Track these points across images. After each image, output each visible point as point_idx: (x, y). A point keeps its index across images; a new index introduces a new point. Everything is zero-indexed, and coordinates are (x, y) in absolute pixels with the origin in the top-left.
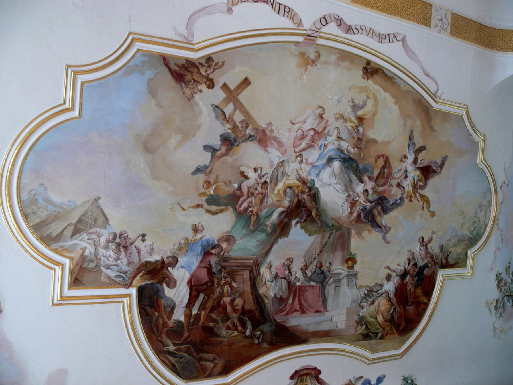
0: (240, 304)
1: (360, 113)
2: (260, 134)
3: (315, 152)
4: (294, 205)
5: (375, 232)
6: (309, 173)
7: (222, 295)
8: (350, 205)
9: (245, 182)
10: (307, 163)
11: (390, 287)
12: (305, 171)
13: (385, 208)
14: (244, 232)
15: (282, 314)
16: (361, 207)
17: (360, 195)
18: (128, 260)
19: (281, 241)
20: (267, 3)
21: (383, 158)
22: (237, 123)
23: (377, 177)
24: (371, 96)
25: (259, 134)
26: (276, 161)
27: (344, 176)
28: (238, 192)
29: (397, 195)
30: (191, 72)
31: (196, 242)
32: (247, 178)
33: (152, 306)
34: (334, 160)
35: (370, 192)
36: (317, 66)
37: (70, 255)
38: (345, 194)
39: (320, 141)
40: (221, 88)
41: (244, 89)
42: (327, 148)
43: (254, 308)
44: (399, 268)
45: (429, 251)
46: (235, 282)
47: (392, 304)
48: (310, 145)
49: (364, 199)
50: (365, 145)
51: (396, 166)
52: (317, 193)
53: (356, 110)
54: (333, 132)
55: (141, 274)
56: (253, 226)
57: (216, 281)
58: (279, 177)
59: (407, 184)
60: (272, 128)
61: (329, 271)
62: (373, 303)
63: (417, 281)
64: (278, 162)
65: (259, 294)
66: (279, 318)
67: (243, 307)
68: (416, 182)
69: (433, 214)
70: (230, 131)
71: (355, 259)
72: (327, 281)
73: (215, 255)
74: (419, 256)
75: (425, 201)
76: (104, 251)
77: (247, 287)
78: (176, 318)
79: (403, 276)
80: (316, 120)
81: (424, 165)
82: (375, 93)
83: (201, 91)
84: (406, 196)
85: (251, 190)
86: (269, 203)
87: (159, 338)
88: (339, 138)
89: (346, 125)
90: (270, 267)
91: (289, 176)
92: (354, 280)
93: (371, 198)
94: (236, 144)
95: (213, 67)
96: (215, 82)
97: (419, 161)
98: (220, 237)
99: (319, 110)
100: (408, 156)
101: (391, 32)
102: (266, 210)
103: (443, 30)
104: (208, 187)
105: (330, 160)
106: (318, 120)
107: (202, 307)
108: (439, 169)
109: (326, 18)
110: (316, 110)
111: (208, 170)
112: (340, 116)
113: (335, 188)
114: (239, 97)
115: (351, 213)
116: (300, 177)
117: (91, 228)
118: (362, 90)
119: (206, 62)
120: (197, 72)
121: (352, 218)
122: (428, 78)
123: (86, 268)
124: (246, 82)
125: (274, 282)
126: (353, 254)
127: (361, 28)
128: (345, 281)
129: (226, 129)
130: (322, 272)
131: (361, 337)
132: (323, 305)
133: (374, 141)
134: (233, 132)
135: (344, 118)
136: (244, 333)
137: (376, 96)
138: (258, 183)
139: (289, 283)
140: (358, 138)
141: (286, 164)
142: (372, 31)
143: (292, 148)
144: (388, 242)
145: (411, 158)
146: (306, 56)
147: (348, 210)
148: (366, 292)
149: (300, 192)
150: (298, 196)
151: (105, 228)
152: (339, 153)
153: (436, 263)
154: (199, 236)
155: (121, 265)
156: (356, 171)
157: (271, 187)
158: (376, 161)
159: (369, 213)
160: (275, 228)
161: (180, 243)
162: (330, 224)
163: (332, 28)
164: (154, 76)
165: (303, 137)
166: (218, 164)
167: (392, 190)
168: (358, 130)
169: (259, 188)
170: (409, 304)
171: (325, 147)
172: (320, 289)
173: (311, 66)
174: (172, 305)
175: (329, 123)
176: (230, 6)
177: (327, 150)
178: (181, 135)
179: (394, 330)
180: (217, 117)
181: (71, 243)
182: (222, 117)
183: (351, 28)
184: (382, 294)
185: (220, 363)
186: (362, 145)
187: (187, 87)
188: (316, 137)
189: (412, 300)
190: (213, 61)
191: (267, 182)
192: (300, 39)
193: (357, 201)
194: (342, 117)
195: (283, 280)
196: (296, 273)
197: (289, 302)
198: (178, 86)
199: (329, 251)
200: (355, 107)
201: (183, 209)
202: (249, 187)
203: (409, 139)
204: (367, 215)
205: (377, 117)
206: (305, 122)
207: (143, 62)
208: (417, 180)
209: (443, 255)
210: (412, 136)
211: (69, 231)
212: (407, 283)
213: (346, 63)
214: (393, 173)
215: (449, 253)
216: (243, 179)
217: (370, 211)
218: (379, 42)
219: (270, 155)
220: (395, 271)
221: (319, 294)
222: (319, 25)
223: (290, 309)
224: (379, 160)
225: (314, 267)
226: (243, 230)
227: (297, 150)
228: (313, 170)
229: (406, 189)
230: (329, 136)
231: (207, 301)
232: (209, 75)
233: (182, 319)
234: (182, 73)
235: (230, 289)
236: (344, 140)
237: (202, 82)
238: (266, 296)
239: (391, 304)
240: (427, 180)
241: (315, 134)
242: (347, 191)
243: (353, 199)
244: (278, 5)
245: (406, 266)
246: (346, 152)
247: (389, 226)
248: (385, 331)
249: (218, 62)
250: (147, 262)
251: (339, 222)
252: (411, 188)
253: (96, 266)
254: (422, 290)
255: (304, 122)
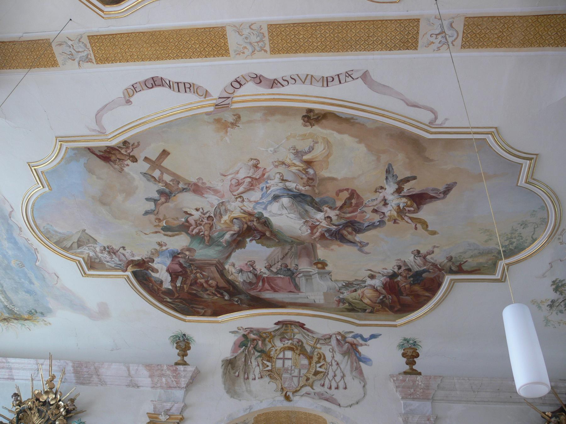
0: (214, 283)
1: (306, 157)
2: (193, 187)
3: (256, 193)
4: (244, 229)
5: (346, 246)
6: (254, 208)
7: (196, 279)
8: (309, 228)
9: (190, 218)
10: (250, 201)
11: (377, 282)
12: (249, 207)
13: (357, 229)
14: (201, 246)
15: (254, 291)
16: (324, 229)
17: (321, 221)
18: (119, 259)
19: (238, 251)
20: (163, 86)
21: (348, 192)
22: (168, 182)
23: (341, 208)
24: (320, 140)
25: (191, 186)
26: (216, 203)
27: (297, 208)
28: (187, 224)
29: (373, 219)
30: (114, 154)
31: (163, 251)
32: (191, 215)
33: (146, 280)
34: (281, 197)
35: (334, 218)
36: (238, 126)
37: (82, 256)
38: (301, 220)
39: (260, 185)
40: (143, 160)
41: (164, 159)
42: (270, 189)
43: (227, 286)
44: (385, 271)
45: (428, 261)
46: (205, 272)
47: (380, 293)
48: (249, 189)
49: (327, 223)
50: (318, 183)
51: (368, 197)
52: (268, 221)
53: (300, 155)
54: (274, 177)
55: (131, 265)
56: (208, 242)
57: (188, 270)
58: (222, 212)
59: (390, 211)
60: (203, 181)
61: (297, 270)
62: (355, 291)
63: (413, 281)
64: (218, 203)
65: (228, 279)
66: (253, 293)
67: (217, 285)
68: (401, 208)
69: (434, 233)
70: (164, 188)
71: (325, 263)
72: (295, 275)
73: (182, 257)
74: (413, 264)
75: (420, 223)
76: (102, 255)
77: (217, 275)
78: (165, 287)
79: (394, 276)
80: (250, 170)
81: (414, 193)
82: (325, 137)
83: (128, 165)
84: (388, 219)
85: (198, 222)
86: (218, 229)
87: (158, 295)
88: (283, 180)
89: (290, 169)
90: (233, 265)
91: (232, 211)
92: (328, 276)
93: (337, 223)
94: (173, 195)
95: (131, 148)
96: (136, 157)
97: (405, 190)
98: (182, 248)
99: (252, 162)
100: (387, 187)
101: (342, 70)
102: (217, 233)
103: (445, 47)
104: (160, 222)
105: (276, 198)
106: (252, 170)
107: (183, 283)
108: (442, 195)
109: (239, 81)
110: (248, 162)
111: (156, 212)
112: (280, 163)
113: (288, 217)
114: (162, 164)
115: (312, 233)
116: (245, 211)
117: (87, 244)
118: (304, 137)
119: (124, 145)
120: (119, 153)
121: (315, 236)
122: (416, 108)
123: (94, 262)
124: (165, 153)
125: (240, 274)
126: (321, 260)
127: (292, 78)
128: (317, 275)
129: (161, 186)
130: (289, 270)
131: (344, 310)
132: (295, 288)
133: (332, 179)
134: (167, 188)
135: (285, 165)
136: (224, 298)
137: (327, 139)
138: (203, 218)
139: (256, 275)
140: (309, 178)
141: (227, 204)
142: (309, 77)
143: (230, 192)
144: (367, 253)
145: (391, 188)
146: (223, 121)
147: (307, 232)
148: (344, 284)
149: (248, 221)
150: (247, 223)
151: (97, 244)
152: (285, 191)
153: (440, 270)
154: (164, 248)
155: (115, 261)
156: (311, 203)
157: (217, 219)
158: (337, 194)
159: (336, 233)
160: (229, 244)
161: (152, 252)
162: (290, 241)
163: (250, 88)
164: (87, 161)
165: (239, 184)
166: (162, 209)
167: (366, 216)
168: (307, 172)
169: (205, 221)
170: (404, 295)
171: (268, 189)
172: (290, 279)
173: (232, 128)
174: (160, 281)
175: (268, 170)
176: (127, 98)
177: (270, 191)
178: (125, 194)
179: (387, 309)
180: (148, 180)
181: (79, 250)
182: (153, 180)
183: (276, 82)
184: (365, 286)
185: (209, 311)
186: (316, 183)
187: (115, 164)
188: (255, 182)
189: (408, 293)
190: (129, 143)
191: (212, 217)
192: (211, 109)
193: (318, 225)
194: (283, 163)
195: (249, 273)
196: (261, 270)
197: (259, 285)
198: (108, 164)
199: (293, 257)
200: (298, 153)
201: (145, 234)
202: (195, 220)
203: (387, 172)
204: (334, 235)
205: (331, 158)
206: (238, 173)
207: (75, 154)
208: (403, 207)
209: (453, 263)
210: (391, 169)
211: (75, 245)
212: (398, 281)
213: (278, 117)
214: (365, 202)
215: (462, 263)
216: (188, 216)
217: (336, 231)
218: (323, 86)
219: (207, 199)
220: (379, 273)
221: (290, 282)
222: (231, 90)
223: (262, 289)
224: (341, 194)
225: (279, 266)
226: (200, 245)
227: (234, 193)
228: (258, 206)
229: (388, 214)
230: (271, 180)
231: (186, 281)
232: (129, 153)
233: (170, 287)
234: (107, 156)
235: (202, 276)
236: (290, 182)
237: (126, 159)
238: (235, 281)
239: (378, 293)
240: (422, 206)
241: (252, 180)
242: (303, 218)
243: (312, 224)
244: (176, 85)
245: (396, 270)
246: (294, 190)
247: (366, 242)
248: (375, 309)
249: (134, 143)
250: (132, 260)
251: (299, 239)
252: (395, 214)
253: (100, 261)
254: (422, 288)
255: (237, 172)
